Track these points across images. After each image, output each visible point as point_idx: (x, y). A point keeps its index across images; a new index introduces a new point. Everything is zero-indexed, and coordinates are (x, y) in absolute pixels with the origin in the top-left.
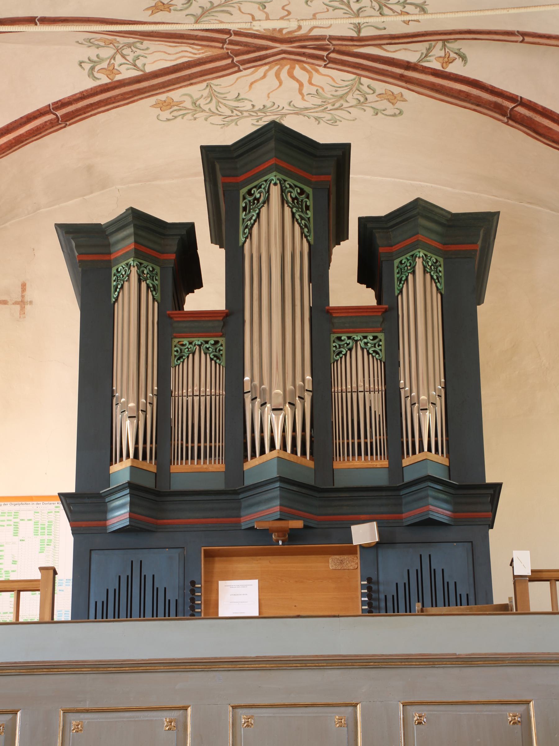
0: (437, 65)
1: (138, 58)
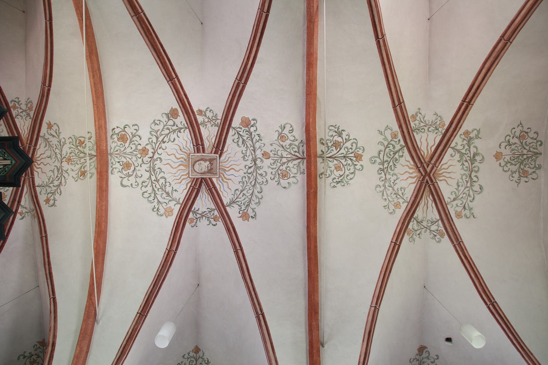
0: (20, 210)
1: (21, 116)
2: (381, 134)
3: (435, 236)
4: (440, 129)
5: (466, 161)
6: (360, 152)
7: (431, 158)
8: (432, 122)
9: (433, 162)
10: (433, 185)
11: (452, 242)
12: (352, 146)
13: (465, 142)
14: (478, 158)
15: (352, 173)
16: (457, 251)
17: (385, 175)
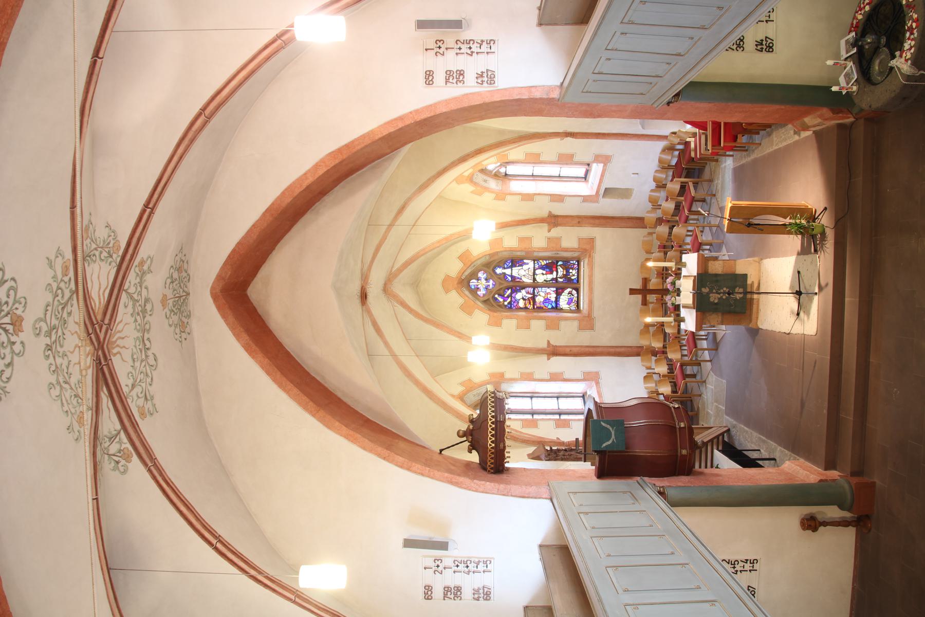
2: (51, 267)
3: (118, 462)
4: (115, 256)
5: (138, 314)
6: (19, 312)
7: (105, 314)
8: (104, 241)
9: (106, 321)
10: (108, 365)
11: (145, 464)
12: (8, 296)
13: (138, 280)
14: (149, 307)
15: (9, 365)
16: (154, 478)
17: (54, 357)
